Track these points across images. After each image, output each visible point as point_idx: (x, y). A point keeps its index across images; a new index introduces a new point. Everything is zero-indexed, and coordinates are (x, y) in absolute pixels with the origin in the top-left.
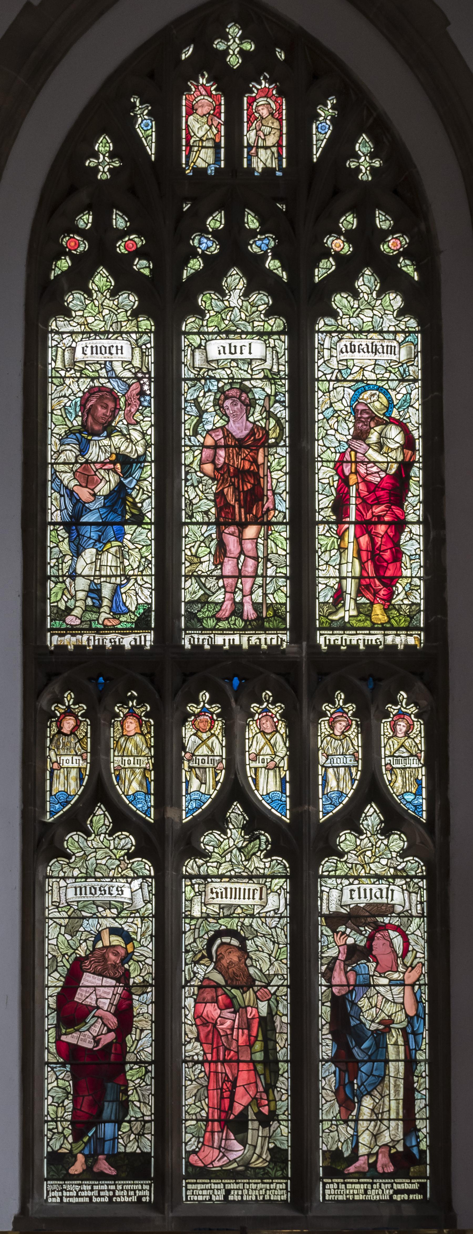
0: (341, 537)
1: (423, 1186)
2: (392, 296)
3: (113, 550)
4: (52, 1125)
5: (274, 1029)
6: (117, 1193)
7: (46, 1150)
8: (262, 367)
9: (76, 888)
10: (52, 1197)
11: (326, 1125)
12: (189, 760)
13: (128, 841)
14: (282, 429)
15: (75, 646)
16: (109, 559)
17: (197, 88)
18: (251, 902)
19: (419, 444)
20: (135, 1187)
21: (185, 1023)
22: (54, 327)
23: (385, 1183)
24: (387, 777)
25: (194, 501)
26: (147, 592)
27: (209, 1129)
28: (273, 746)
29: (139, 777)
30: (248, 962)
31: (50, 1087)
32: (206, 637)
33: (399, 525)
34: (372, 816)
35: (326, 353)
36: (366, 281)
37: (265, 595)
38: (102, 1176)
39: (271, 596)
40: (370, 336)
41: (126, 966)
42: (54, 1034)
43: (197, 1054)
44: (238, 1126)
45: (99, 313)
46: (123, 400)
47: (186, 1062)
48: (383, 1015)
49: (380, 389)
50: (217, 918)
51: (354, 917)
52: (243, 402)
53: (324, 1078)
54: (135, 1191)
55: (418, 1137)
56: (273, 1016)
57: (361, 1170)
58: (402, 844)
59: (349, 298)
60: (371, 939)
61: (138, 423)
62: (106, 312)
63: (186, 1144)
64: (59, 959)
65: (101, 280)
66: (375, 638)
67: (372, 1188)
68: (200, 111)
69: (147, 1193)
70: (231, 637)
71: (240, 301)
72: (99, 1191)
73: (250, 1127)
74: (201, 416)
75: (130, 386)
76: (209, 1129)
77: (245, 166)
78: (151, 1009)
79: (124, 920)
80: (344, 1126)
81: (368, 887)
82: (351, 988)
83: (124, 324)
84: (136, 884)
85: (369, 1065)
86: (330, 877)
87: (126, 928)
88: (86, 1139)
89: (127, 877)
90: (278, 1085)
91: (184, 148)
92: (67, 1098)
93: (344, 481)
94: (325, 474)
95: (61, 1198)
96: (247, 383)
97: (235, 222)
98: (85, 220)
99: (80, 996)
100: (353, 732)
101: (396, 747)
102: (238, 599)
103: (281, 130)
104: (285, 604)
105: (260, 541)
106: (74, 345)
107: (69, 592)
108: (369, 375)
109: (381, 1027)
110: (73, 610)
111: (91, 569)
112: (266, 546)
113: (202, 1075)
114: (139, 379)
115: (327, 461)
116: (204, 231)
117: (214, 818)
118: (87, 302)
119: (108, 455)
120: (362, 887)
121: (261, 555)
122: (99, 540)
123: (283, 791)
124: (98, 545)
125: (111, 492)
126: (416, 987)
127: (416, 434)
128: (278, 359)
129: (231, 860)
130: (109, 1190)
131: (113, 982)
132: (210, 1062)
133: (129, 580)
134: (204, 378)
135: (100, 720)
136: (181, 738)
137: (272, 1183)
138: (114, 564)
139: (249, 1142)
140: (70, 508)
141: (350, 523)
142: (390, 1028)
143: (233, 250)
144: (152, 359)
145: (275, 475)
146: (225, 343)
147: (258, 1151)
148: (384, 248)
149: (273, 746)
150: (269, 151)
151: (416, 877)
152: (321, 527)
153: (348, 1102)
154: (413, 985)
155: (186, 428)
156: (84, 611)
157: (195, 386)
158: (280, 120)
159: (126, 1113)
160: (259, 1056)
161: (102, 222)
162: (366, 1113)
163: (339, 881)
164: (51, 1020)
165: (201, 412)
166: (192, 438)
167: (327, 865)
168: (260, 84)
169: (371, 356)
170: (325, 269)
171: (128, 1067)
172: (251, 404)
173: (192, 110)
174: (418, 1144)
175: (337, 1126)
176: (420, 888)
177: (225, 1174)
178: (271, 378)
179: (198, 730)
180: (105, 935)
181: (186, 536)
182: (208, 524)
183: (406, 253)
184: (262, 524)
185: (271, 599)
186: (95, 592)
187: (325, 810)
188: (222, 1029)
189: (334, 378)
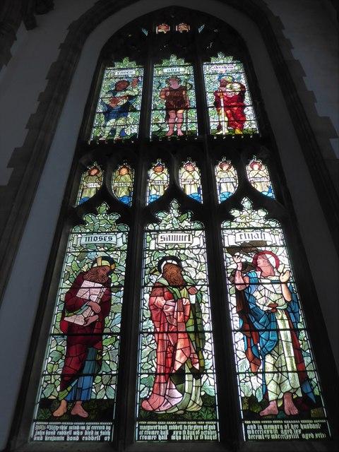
0: (219, 111)
1: (324, 425)
4: (48, 378)
5: (200, 311)
6: (86, 433)
7: (39, 397)
10: (38, 436)
16: (121, 121)
18: (184, 242)
20: (100, 428)
21: (143, 309)
23: (293, 424)
27: (157, 381)
30: (183, 273)
38: (76, 419)
43: (150, 328)
44: (179, 377)
47: (143, 333)
48: (270, 301)
50: (164, 250)
51: (244, 248)
53: (237, 343)
54: (99, 431)
55: (311, 385)
56: (199, 304)
57: (273, 413)
60: (255, 259)
63: (140, 392)
67: (284, 428)
72: (73, 431)
73: (187, 379)
76: (157, 381)
80: (255, 377)
81: (250, 233)
82: (247, 286)
84: (120, 234)
86: (227, 229)
87: (112, 256)
89: (114, 232)
90: (206, 348)
92: (61, 358)
95: (44, 436)
99: (80, 294)
102: (175, 130)
112: (187, 115)
117: (163, 204)
123: (199, 193)
126: (289, 284)
129: (172, 223)
130: (80, 430)
132: (158, 333)
137: (205, 424)
139: (187, 390)
142: (277, 309)
151: (276, 227)
154: (286, 283)
155: (154, 88)
160: (191, 329)
162: (269, 367)
164: (58, 310)
171: (104, 337)
175: (250, 377)
185: (189, 129)
187: (221, 199)
188: (167, 312)
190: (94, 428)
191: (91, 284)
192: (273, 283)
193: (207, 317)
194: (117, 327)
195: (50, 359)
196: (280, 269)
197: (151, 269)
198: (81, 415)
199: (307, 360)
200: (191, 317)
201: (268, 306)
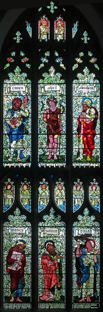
0: (79, 138)
1: (98, 305)
2: (93, 74)
3: (20, 141)
4: (5, 289)
6: (22, 306)
7: (4, 296)
8: (59, 93)
9: (11, 229)
11: (74, 290)
12: (40, 197)
13: (24, 217)
14: (64, 109)
15: (11, 166)
16: (19, 143)
17: (42, 19)
18: (56, 233)
19: (99, 114)
20: (27, 305)
21: (39, 264)
22: (5, 82)
24: (90, 201)
25: (41, 128)
26: (29, 152)
27: (45, 291)
28: (61, 193)
29: (27, 201)
30: (55, 249)
31: (5, 280)
32: (44, 164)
33: (94, 135)
34: (86, 211)
35: (76, 89)
36: (86, 70)
37: (60, 153)
38: (18, 302)
39: (61, 153)
40: (87, 84)
41: (24, 250)
42: (6, 267)
43: (42, 272)
44: (52, 290)
45: (17, 78)
46: (23, 101)
47: (39, 274)
49: (89, 99)
50: (47, 237)
51: (82, 237)
52: (54, 102)
53: (74, 278)
54: (26, 306)
55: (97, 293)
58: (94, 218)
59: (82, 74)
60: (86, 243)
61: (27, 107)
62: (19, 78)
64: (7, 248)
65: (17, 69)
66: (88, 164)
68: (43, 25)
69: (30, 306)
70: (51, 164)
71: (53, 75)
72: (18, 306)
74: (43, 106)
75: (25, 98)
76: (45, 291)
77: (55, 39)
78: (30, 260)
79: (23, 238)
82: (81, 255)
83: (23, 81)
84: (27, 228)
85: (85, 275)
87: (24, 240)
88: (14, 293)
89: (24, 227)
90: (62, 280)
91: (39, 35)
93: (80, 123)
94: (75, 121)
95: (8, 307)
96: (55, 97)
97: (52, 54)
98: (13, 54)
100: (82, 189)
101: (93, 193)
102: (53, 154)
103: (64, 30)
104: (65, 156)
105: (58, 139)
106: (10, 87)
107: (9, 152)
108: (86, 95)
109: (88, 265)
110: (10, 157)
111: (15, 146)
113: (43, 277)
114: (27, 96)
115: (76, 118)
116: (44, 56)
117: (46, 211)
118: (14, 75)
119: (19, 116)
120: (84, 229)
121: (59, 143)
122: (17, 139)
123: (64, 205)
124: (17, 140)
125: (20, 126)
126: (97, 255)
127: (98, 111)
128: (63, 91)
130: (20, 306)
131: (21, 254)
132: (45, 274)
133: (24, 149)
134: (44, 95)
135: (17, 187)
136: (38, 191)
138: (21, 145)
140: (9, 130)
141: (81, 134)
142: (90, 266)
143: (52, 62)
144: (30, 90)
145: (62, 121)
146: (50, 86)
147: (57, 296)
148: (91, 61)
149: (61, 193)
150: (61, 35)
151: (97, 227)
152: (74, 135)
153: (80, 284)
154: (96, 255)
155: (40, 109)
156: (13, 157)
157: (42, 97)
158: (64, 27)
159: (24, 287)
160: (58, 273)
161: (18, 54)
162: (84, 287)
163: (78, 228)
164: (5, 263)
165: (43, 105)
166: (41, 112)
167: (75, 224)
168: (59, 18)
169: (87, 90)
170: (75, 66)
171: (24, 275)
172: (56, 102)
173: (41, 25)
174: (97, 295)
176: (98, 230)
177: (49, 302)
178: (61, 95)
179: (42, 189)
180: (19, 242)
181: (39, 138)
182: (45, 134)
183: (96, 63)
184: (59, 134)
185: (61, 154)
186: (16, 152)
189: (77, 96)
190: (25, 305)
191: (17, 253)
192: (91, 254)
193: (64, 269)
194: (30, 272)
195: (5, 283)
196: (96, 247)
197: (42, 247)
198: (20, 301)
199: (98, 285)
200: (58, 268)
201: (88, 264)
